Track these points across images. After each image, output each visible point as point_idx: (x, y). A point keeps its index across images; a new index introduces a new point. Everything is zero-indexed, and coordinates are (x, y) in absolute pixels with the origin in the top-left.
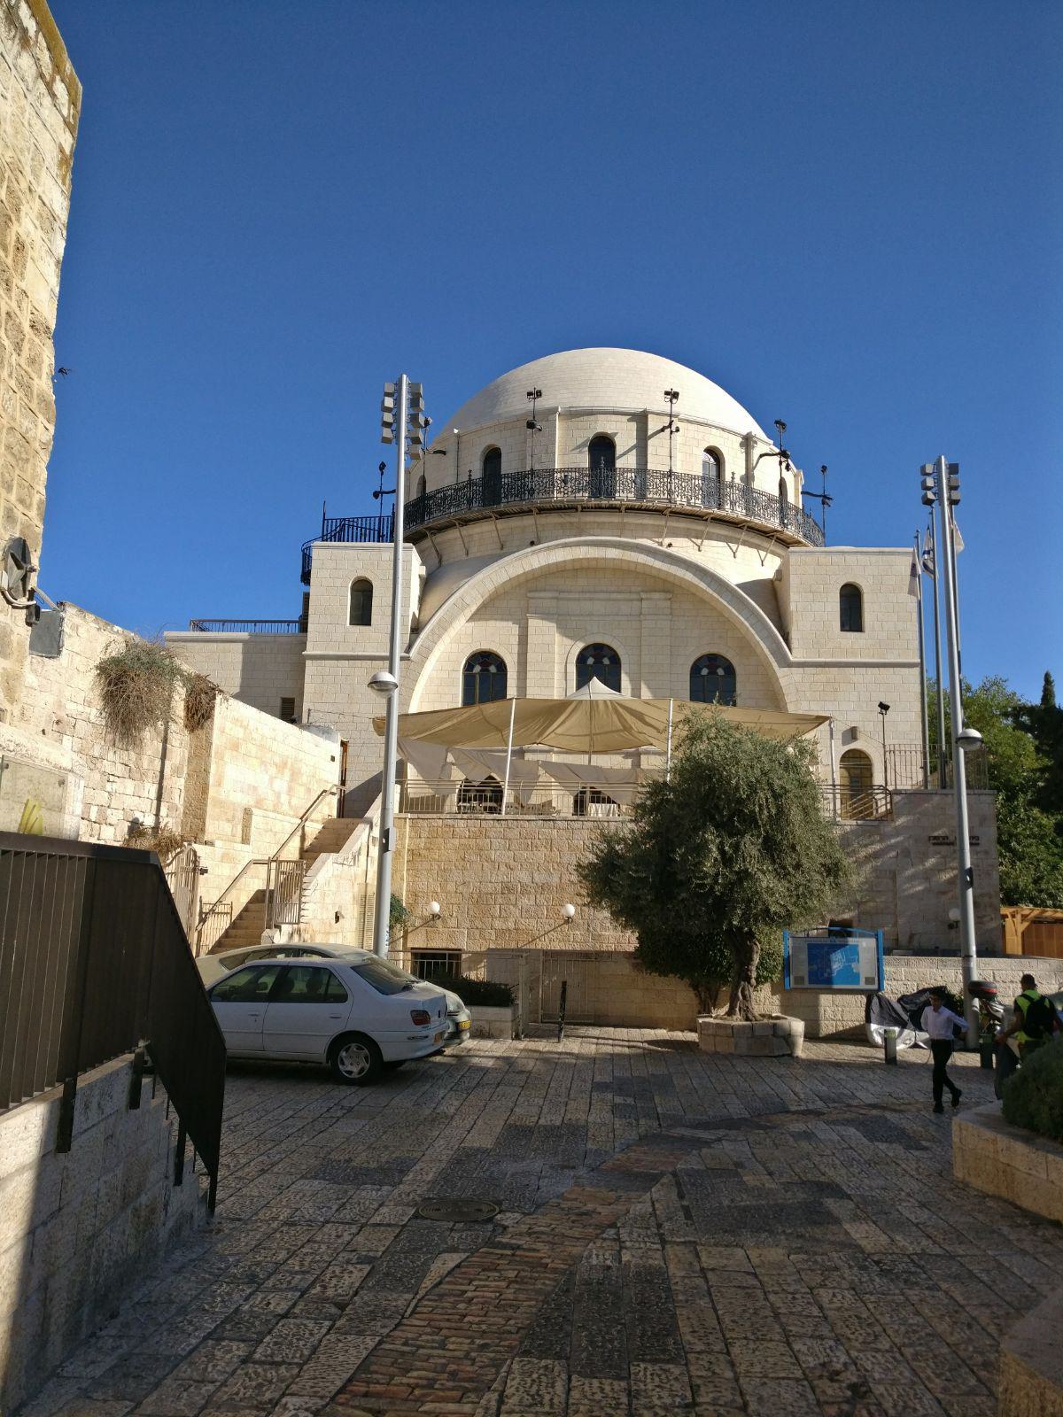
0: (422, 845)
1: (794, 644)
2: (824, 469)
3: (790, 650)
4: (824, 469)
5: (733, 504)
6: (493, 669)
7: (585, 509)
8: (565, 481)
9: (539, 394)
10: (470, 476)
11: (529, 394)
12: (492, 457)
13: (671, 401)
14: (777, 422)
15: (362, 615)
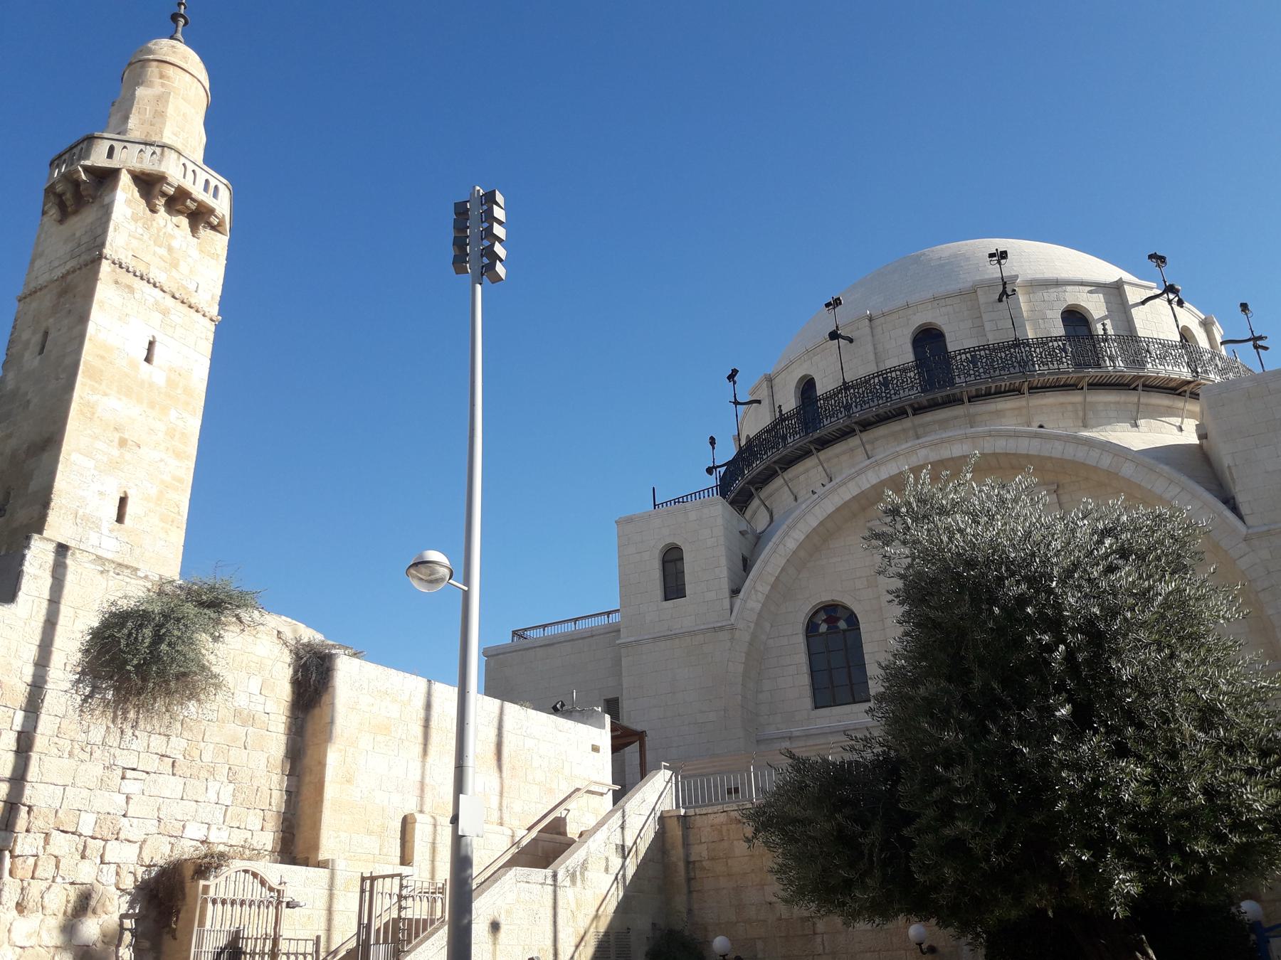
0: (705, 854)
1: (1244, 509)
2: (1244, 307)
3: (1241, 517)
4: (1244, 307)
5: (1112, 359)
6: (842, 625)
7: (919, 409)
8: (885, 383)
9: (837, 302)
10: (780, 411)
11: (827, 305)
12: (807, 385)
13: (999, 262)
14: (1151, 257)
15: (673, 586)
